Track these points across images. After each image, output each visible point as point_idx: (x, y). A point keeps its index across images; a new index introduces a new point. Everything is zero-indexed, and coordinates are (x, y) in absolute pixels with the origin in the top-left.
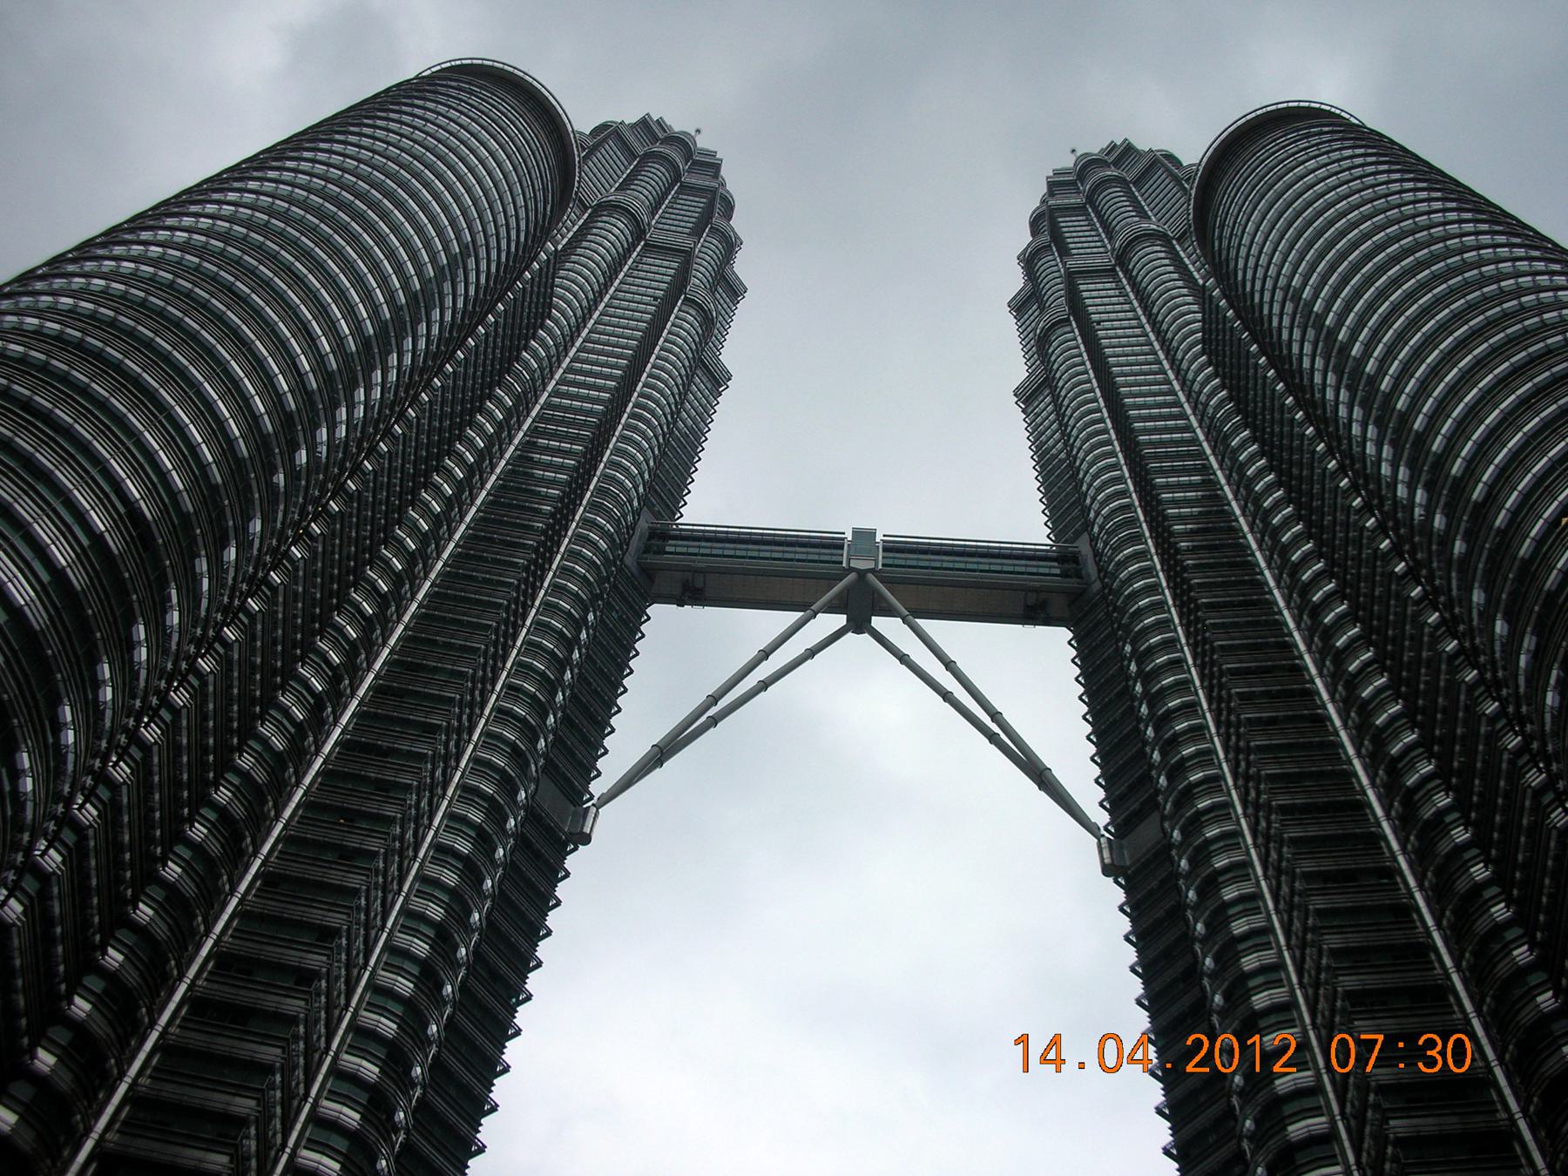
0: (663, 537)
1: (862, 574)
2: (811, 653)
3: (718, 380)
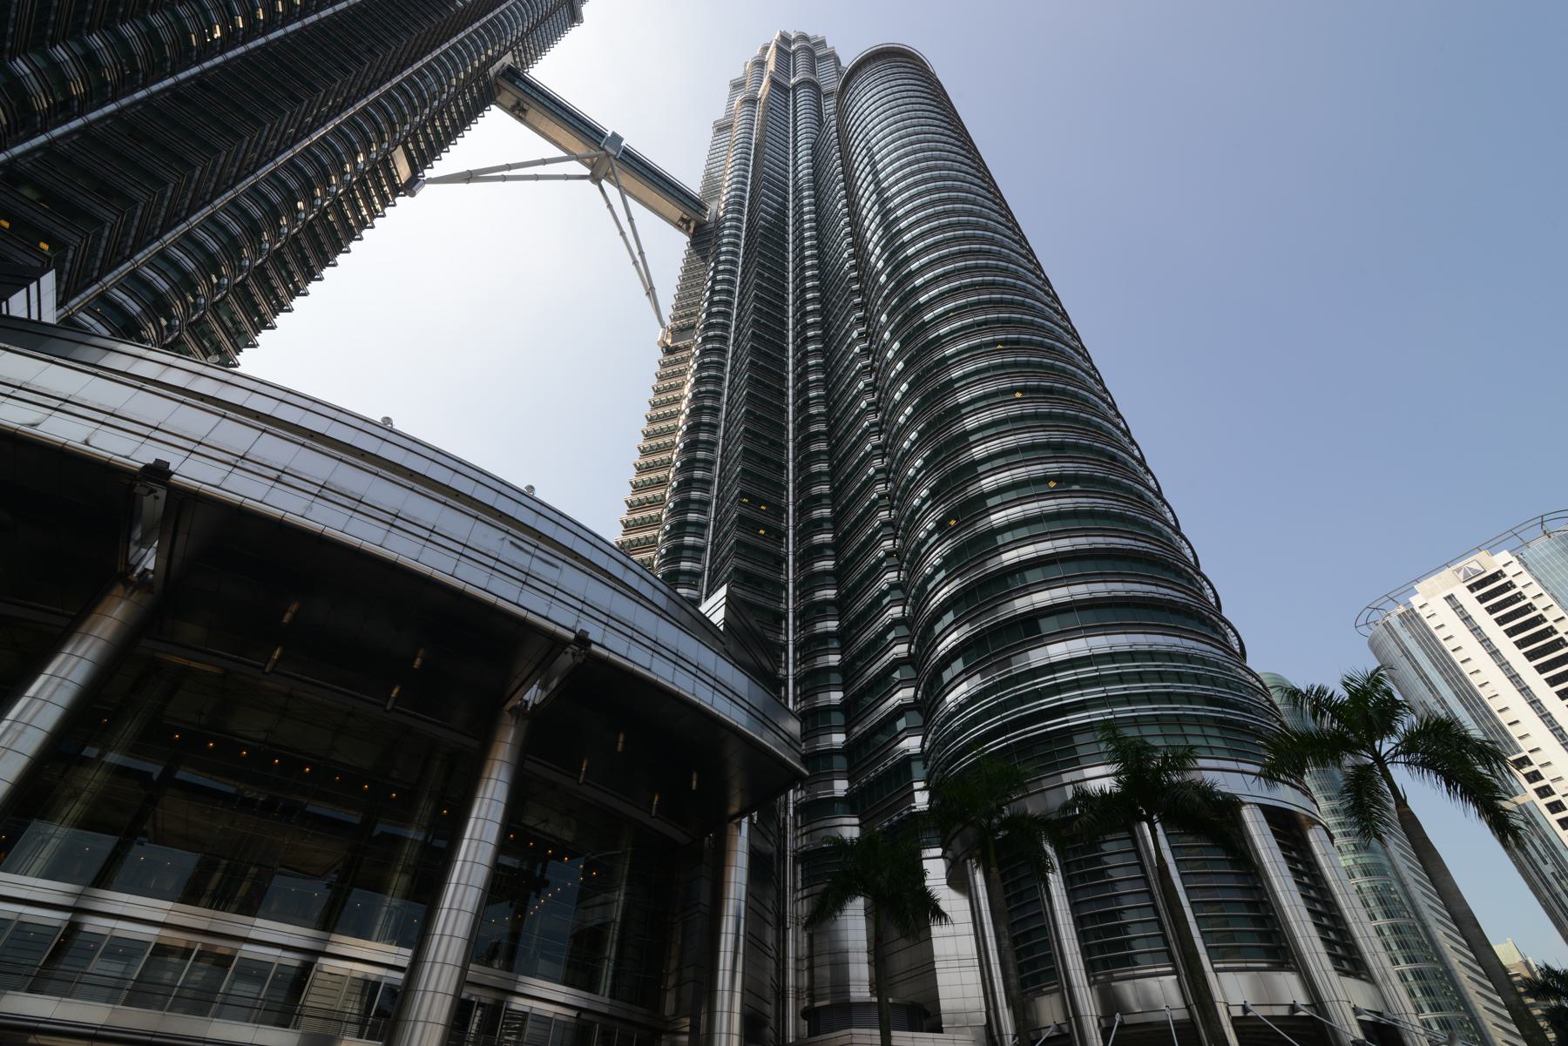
0: (514, 75)
1: (608, 155)
2: (567, 177)
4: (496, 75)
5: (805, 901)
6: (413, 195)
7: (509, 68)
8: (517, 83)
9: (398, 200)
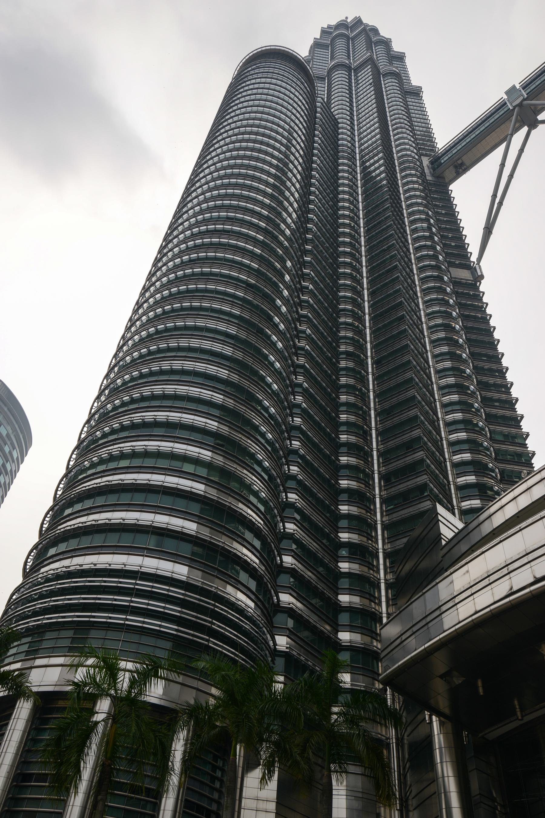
0: (436, 162)
1: (520, 105)
2: (522, 150)
3: (417, 93)
4: (433, 175)
6: (482, 277)
7: (432, 163)
8: (442, 161)
9: (481, 289)
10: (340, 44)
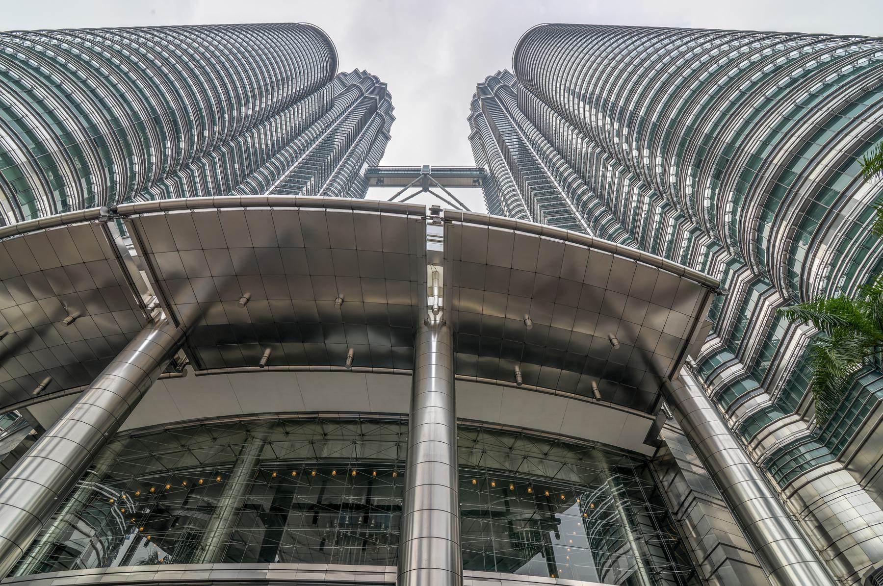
1: (425, 175)
5: (792, 499)
10: (369, 83)
